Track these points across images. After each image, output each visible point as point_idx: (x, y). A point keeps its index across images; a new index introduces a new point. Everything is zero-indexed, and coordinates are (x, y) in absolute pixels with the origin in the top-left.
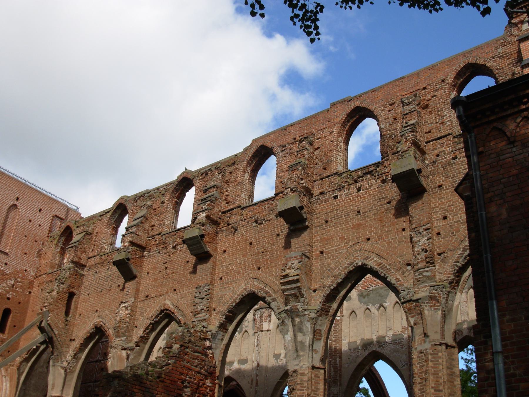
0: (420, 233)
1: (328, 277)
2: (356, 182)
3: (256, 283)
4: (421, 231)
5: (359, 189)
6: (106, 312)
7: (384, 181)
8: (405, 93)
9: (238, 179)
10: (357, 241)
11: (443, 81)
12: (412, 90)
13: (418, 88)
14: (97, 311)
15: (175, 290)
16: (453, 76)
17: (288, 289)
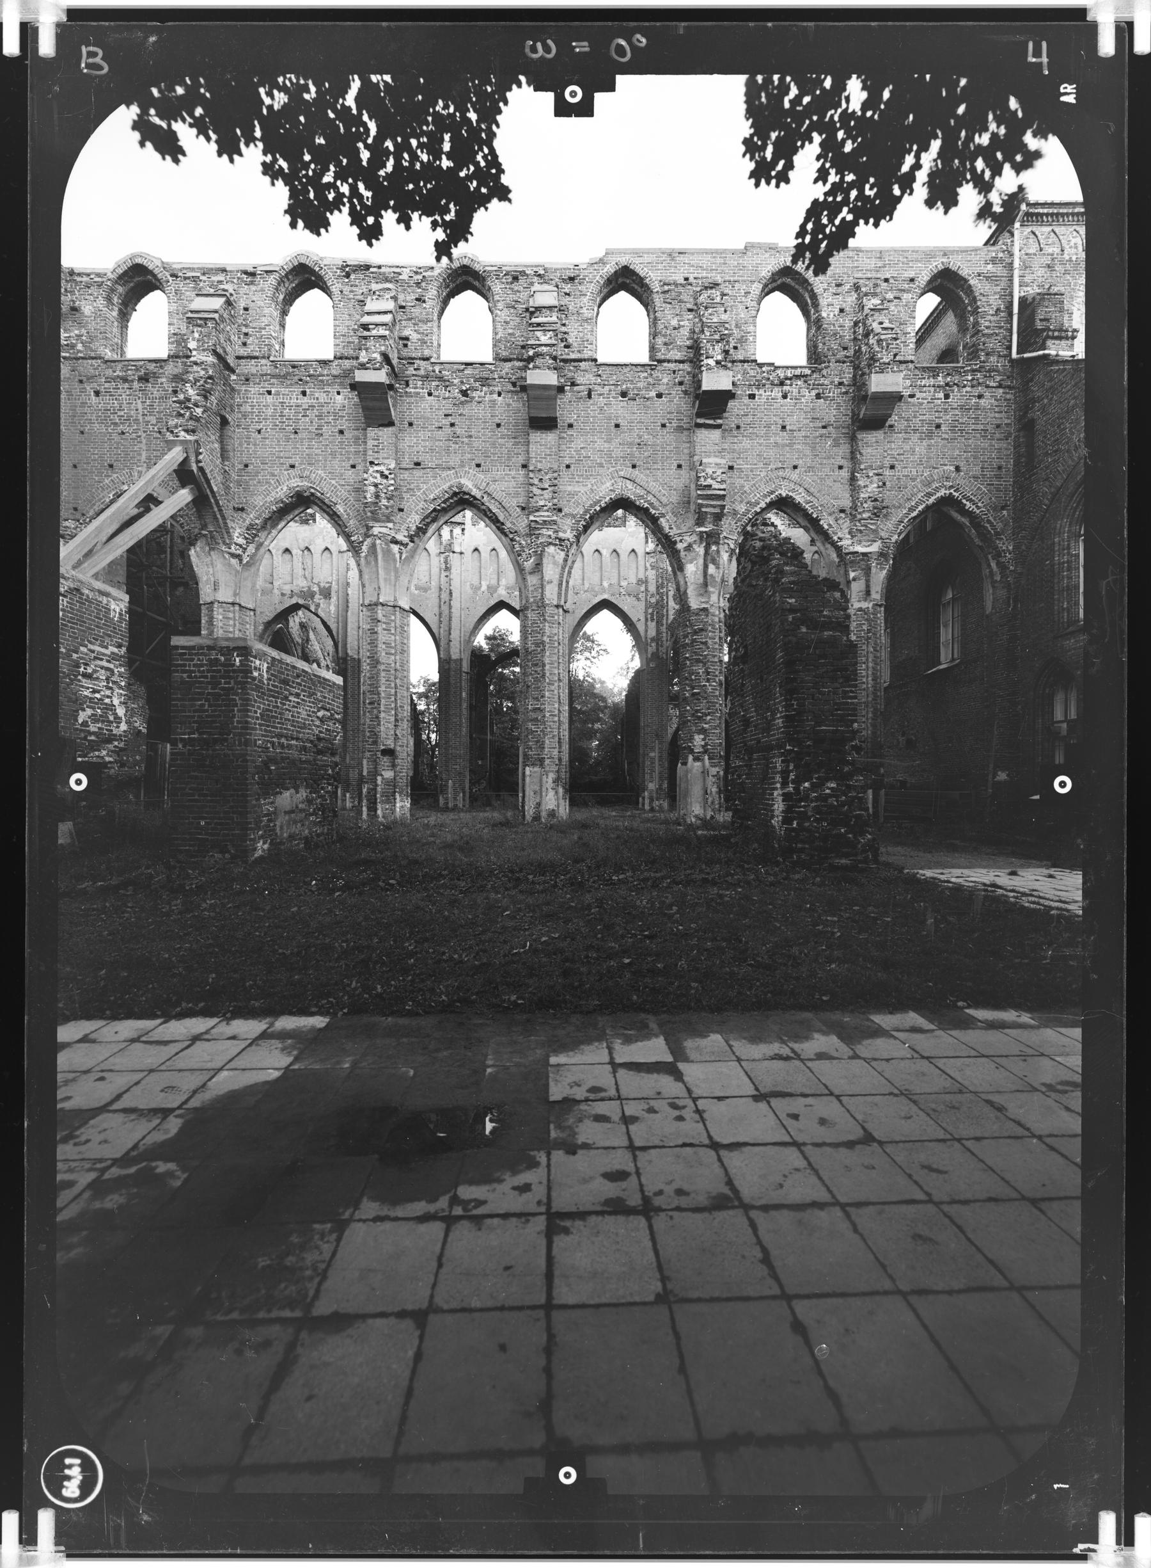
0: (868, 476)
1: (741, 502)
2: (782, 384)
3: (630, 487)
4: (871, 475)
5: (785, 397)
6: (320, 472)
7: (818, 396)
8: (860, 275)
9: (584, 310)
10: (780, 465)
11: (912, 280)
12: (869, 276)
13: (879, 276)
14: (292, 466)
15: (478, 466)
16: (927, 278)
17: (707, 506)
